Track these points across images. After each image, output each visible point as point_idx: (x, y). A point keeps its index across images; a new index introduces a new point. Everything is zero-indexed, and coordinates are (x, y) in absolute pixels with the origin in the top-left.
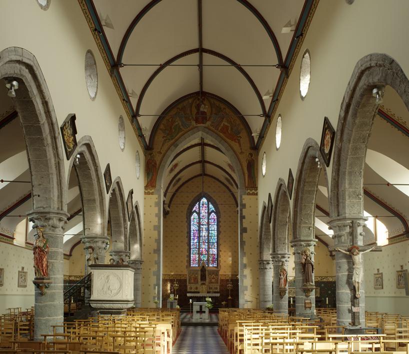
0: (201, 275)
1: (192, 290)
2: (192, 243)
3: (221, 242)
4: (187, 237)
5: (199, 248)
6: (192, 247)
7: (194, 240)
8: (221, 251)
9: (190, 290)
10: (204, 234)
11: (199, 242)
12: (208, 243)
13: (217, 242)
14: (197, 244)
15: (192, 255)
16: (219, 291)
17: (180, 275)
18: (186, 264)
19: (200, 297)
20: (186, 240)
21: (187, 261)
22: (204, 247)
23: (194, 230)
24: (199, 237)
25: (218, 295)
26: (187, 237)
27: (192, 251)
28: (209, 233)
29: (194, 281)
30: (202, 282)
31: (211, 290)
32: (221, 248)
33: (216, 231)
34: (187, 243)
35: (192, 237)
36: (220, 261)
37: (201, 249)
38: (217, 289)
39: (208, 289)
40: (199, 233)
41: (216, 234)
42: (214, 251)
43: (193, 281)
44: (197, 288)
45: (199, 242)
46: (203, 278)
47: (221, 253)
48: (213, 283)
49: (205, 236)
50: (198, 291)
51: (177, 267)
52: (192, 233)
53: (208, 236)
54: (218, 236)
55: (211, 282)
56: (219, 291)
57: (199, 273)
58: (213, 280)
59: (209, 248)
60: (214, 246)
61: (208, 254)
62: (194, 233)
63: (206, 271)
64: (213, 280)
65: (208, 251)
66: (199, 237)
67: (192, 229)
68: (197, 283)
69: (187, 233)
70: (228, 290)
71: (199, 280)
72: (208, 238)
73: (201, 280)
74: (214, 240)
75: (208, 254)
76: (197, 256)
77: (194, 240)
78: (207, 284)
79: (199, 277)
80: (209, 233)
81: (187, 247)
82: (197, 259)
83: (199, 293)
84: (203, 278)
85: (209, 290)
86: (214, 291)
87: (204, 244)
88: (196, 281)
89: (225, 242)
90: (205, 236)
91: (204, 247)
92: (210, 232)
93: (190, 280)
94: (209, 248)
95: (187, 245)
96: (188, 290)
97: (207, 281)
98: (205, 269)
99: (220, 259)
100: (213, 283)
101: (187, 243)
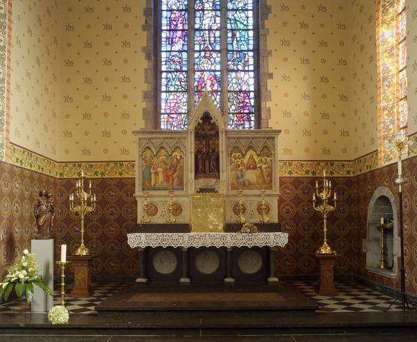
0: (198, 153)
1: (158, 220)
2: (164, 55)
3: (271, 43)
4: (144, 28)
5: (190, 72)
6: (164, 68)
7: (172, 44)
8: (271, 76)
9: (147, 220)
10: (207, 23)
11: (190, 51)
12: (224, 51)
13: (257, 50)
14: (185, 55)
15: (163, 96)
16: (275, 220)
17: (121, 163)
18: (141, 124)
19: (191, 249)
20: (143, 39)
21: (145, 111)
22: (210, 65)
23: (171, 10)
24: (189, 33)
25: (280, 239)
26: (144, 28)
27: (164, 81)
28: (225, 19)
29: (167, 178)
30: (203, 182)
31: (243, 219)
32: (273, 64)
33: (250, 14)
34: (144, 49)
35: (164, 35)
36: (269, 110)
37: (197, 75)
38: (268, 210)
39: (230, 213)
40: (191, 21)
41: (251, 21)
42: (248, 80)
43: (161, 178)
44: (177, 210)
45: (190, 51)
46: (207, 163)
47: (270, 84)
48: (248, 185)
49: (210, 30)
50: (180, 220)
51: (106, 134)
52: (164, 21)
53: (223, 29)
54: (257, 28)
55: (240, 184)
56: (275, 220)
57: (190, 144)
58: (251, 176)
59: (226, 70)
60: (246, 64)
61: (223, 92)
62: (171, 20)
63: (217, 135)
64: (251, 176)
65: (221, 81)
66: (189, 33)
67: (164, 7)
68: (181, 185)
69: (147, 12)
70: (317, 217)
71: (190, 174)
72: (223, 37)
73: (199, 171)
74: (246, 42)
75: (223, 92)
76: (184, 98)
77: (171, 42)
78: (223, 188)
79: (190, 162)
80: (225, 19)
81: (144, 64)
82: (184, 109)
83: (185, 228)
84: (207, 163)
85: (233, 219)
86: (257, 220)
87: (209, 58)
88: (174, 180)
89: (285, 43)
90: (210, 30)
91: (210, 65)
92: (230, 15)
93: (146, 178)
94: (226, 70)
95: (143, 55)
96: (141, 218)
97: (223, 176)
98: (214, 127)
99: (265, 104)
100: (248, 185)
101: (144, 49)
